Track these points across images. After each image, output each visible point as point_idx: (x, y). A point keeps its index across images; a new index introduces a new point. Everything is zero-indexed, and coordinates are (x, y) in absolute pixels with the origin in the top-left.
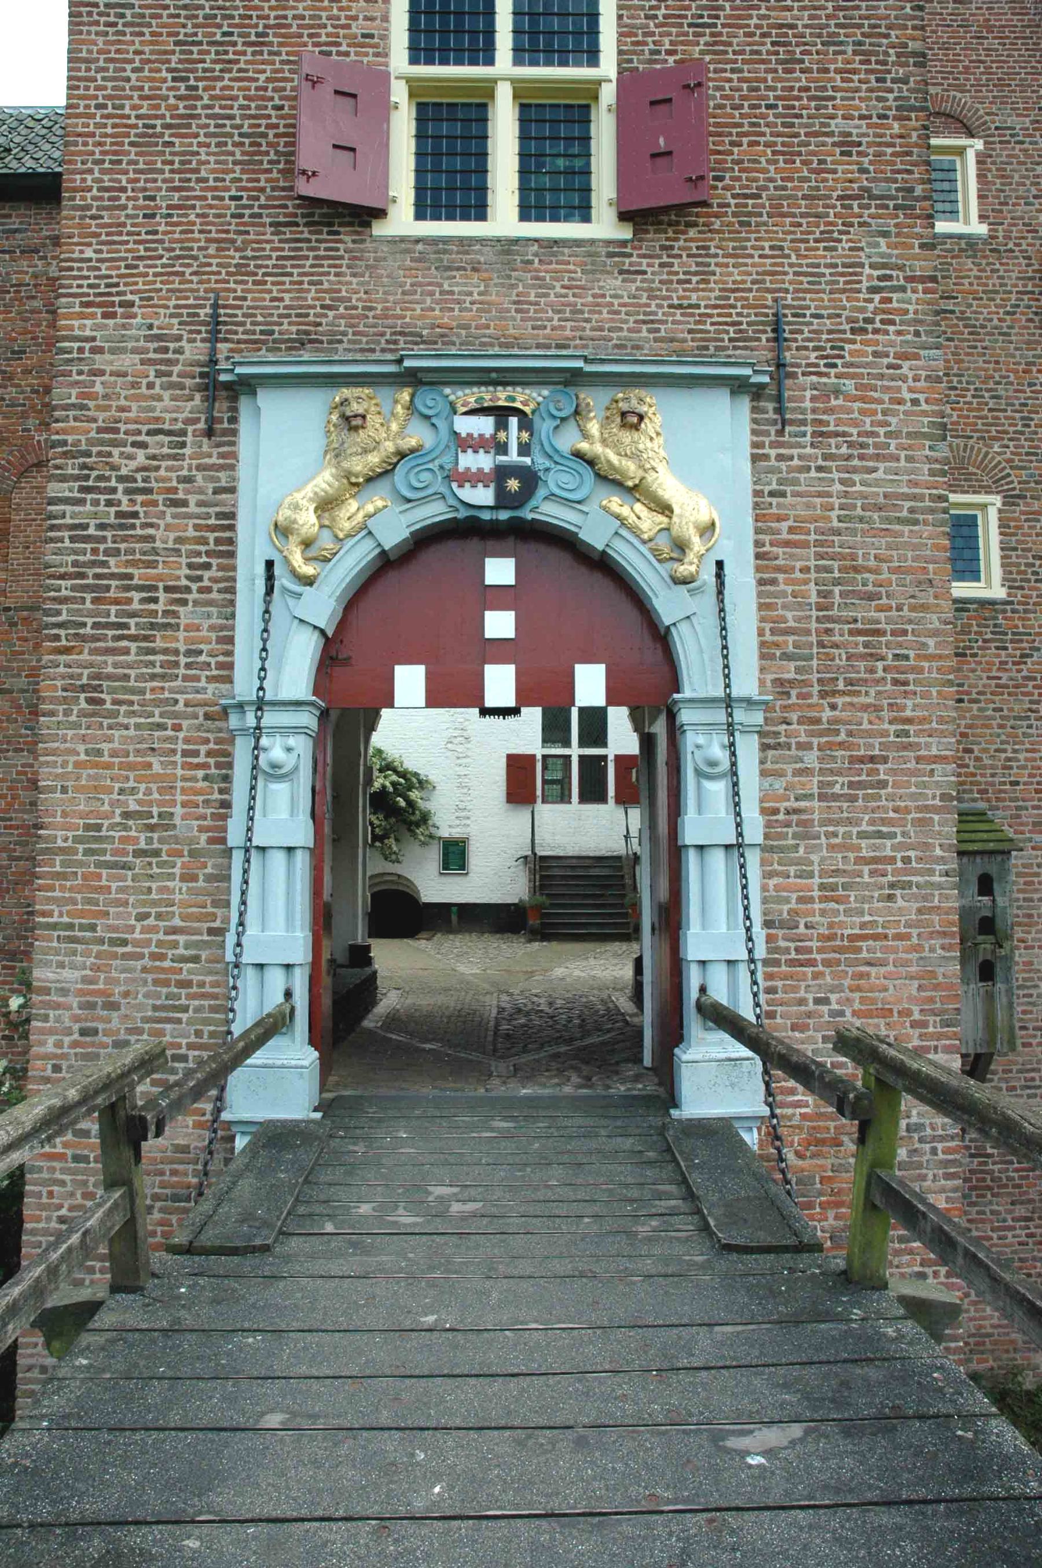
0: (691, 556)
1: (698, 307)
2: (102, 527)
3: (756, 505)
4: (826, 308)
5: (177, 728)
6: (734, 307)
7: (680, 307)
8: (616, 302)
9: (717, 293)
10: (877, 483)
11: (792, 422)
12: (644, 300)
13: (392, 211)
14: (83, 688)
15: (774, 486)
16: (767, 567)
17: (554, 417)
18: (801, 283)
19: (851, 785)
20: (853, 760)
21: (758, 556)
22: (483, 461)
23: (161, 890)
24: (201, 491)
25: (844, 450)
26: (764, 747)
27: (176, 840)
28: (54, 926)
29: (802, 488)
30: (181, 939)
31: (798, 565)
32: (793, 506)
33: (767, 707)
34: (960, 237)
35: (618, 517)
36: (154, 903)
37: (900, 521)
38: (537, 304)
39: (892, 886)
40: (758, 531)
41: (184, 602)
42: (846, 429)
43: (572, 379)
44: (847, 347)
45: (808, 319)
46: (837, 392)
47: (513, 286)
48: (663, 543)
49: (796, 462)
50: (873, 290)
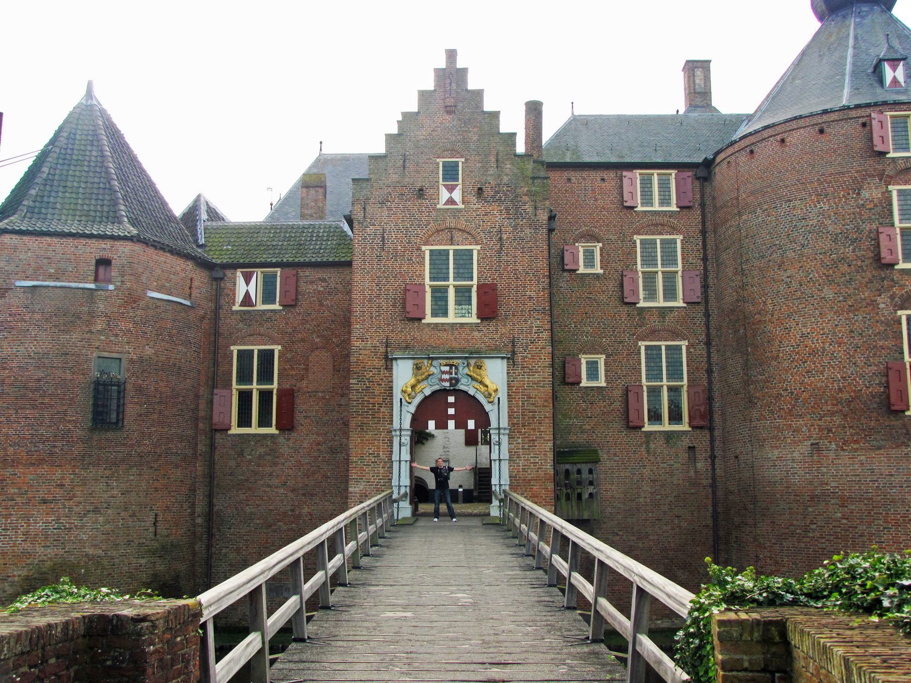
0: (492, 397)
2: (362, 390)
3: (508, 384)
5: (381, 435)
10: (535, 378)
11: (516, 365)
13: (427, 317)
14: (359, 426)
19: (529, 446)
20: (529, 441)
21: (508, 395)
22: (447, 377)
23: (377, 470)
24: (385, 382)
25: (528, 371)
26: (509, 438)
27: (381, 459)
28: (354, 479)
30: (382, 481)
31: (517, 397)
34: (594, 274)
35: (476, 388)
36: (376, 473)
37: (540, 387)
39: (538, 468)
40: (508, 390)
41: (382, 407)
46: (526, 357)
50: (535, 333)
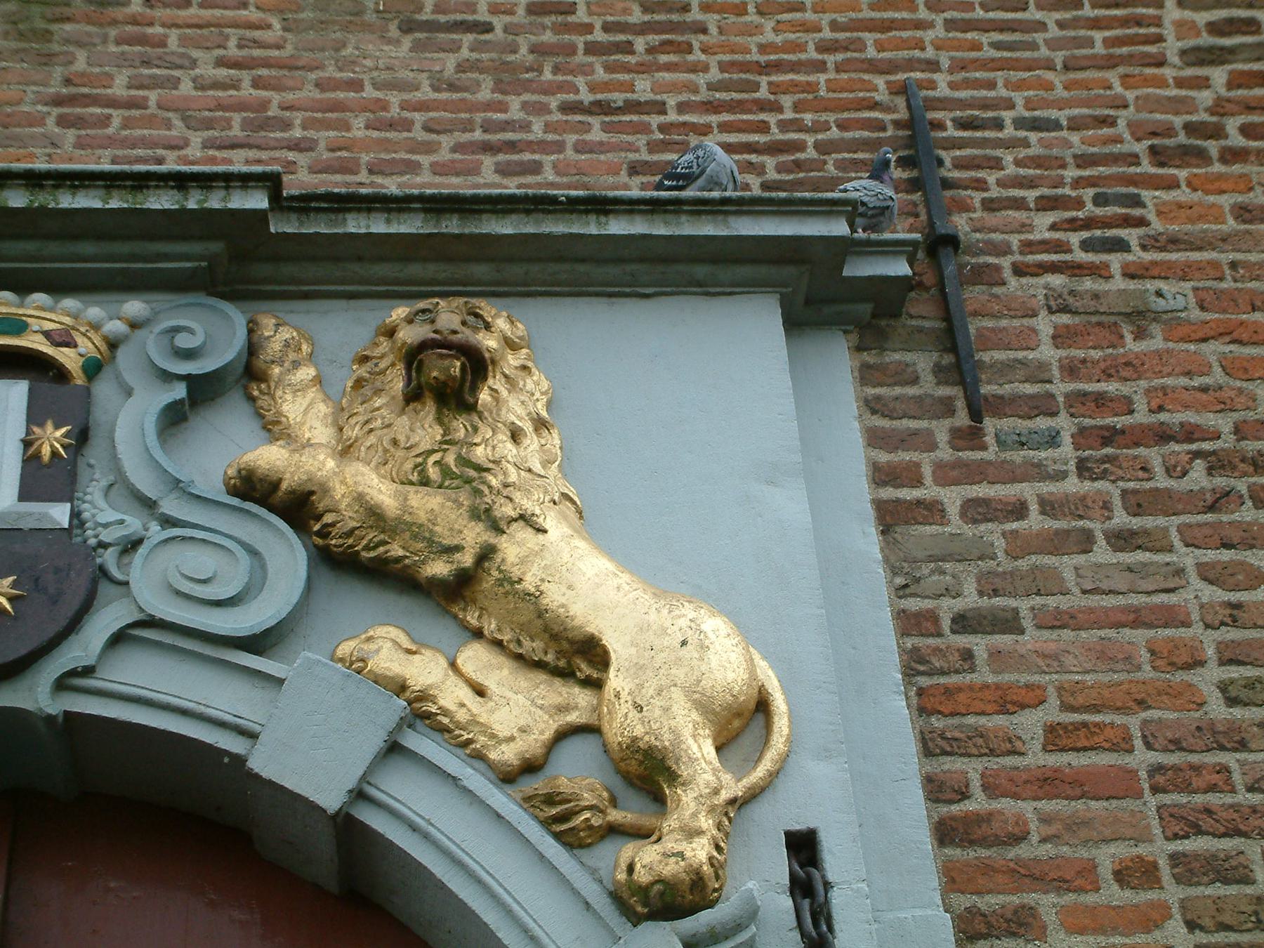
1: (661, 108)
3: (914, 665)
4: (1061, 105)
6: (776, 108)
7: (601, 108)
8: (394, 99)
9: (715, 74)
11: (1001, 406)
12: (485, 94)
15: (970, 599)
16: (987, 869)
17: (167, 377)
18: (977, 47)
21: (945, 833)
25: (1198, 477)
29: (1073, 601)
31: (1107, 857)
32: (1053, 659)
35: (400, 687)
38: (131, 104)
40: (930, 747)
42: (1191, 417)
44: (1146, 195)
45: (1009, 131)
46: (1140, 318)
47: (47, 59)
49: (1035, 521)
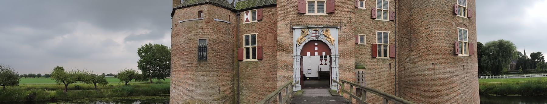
13: (306, 13)
22: (315, 35)
33: (339, 55)
43: (322, 28)
48: (330, 41)
